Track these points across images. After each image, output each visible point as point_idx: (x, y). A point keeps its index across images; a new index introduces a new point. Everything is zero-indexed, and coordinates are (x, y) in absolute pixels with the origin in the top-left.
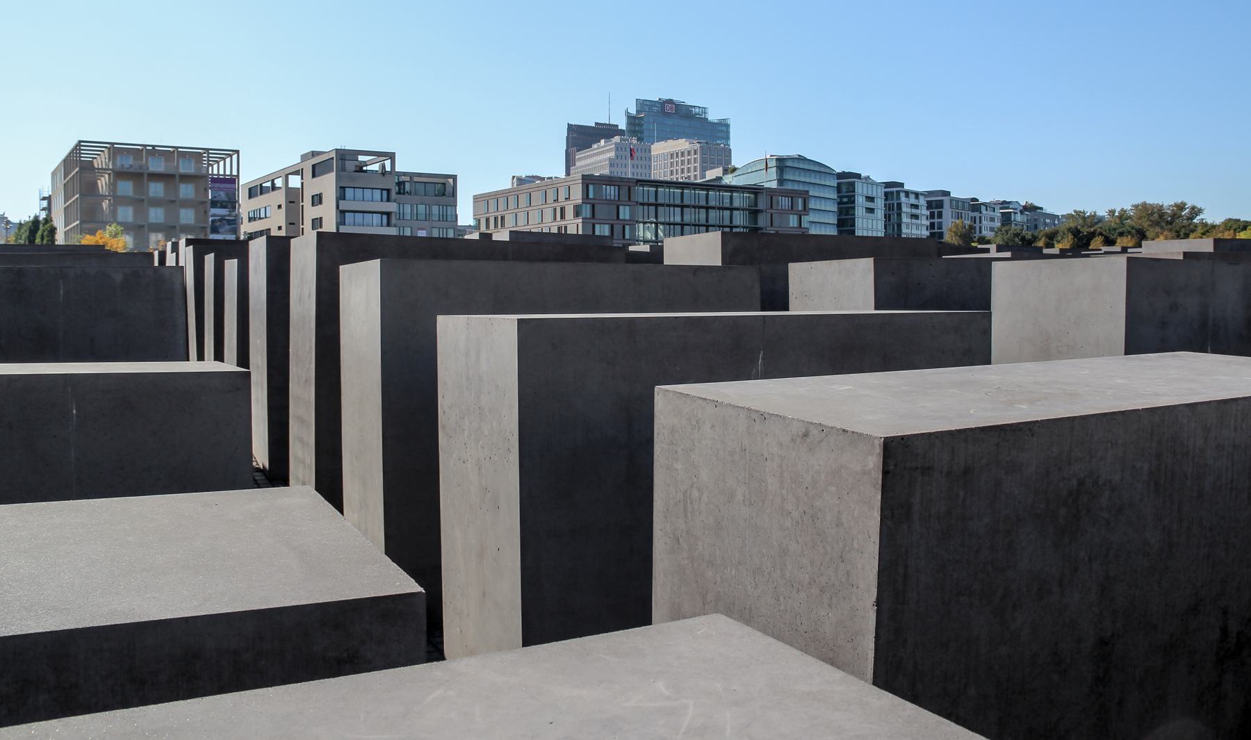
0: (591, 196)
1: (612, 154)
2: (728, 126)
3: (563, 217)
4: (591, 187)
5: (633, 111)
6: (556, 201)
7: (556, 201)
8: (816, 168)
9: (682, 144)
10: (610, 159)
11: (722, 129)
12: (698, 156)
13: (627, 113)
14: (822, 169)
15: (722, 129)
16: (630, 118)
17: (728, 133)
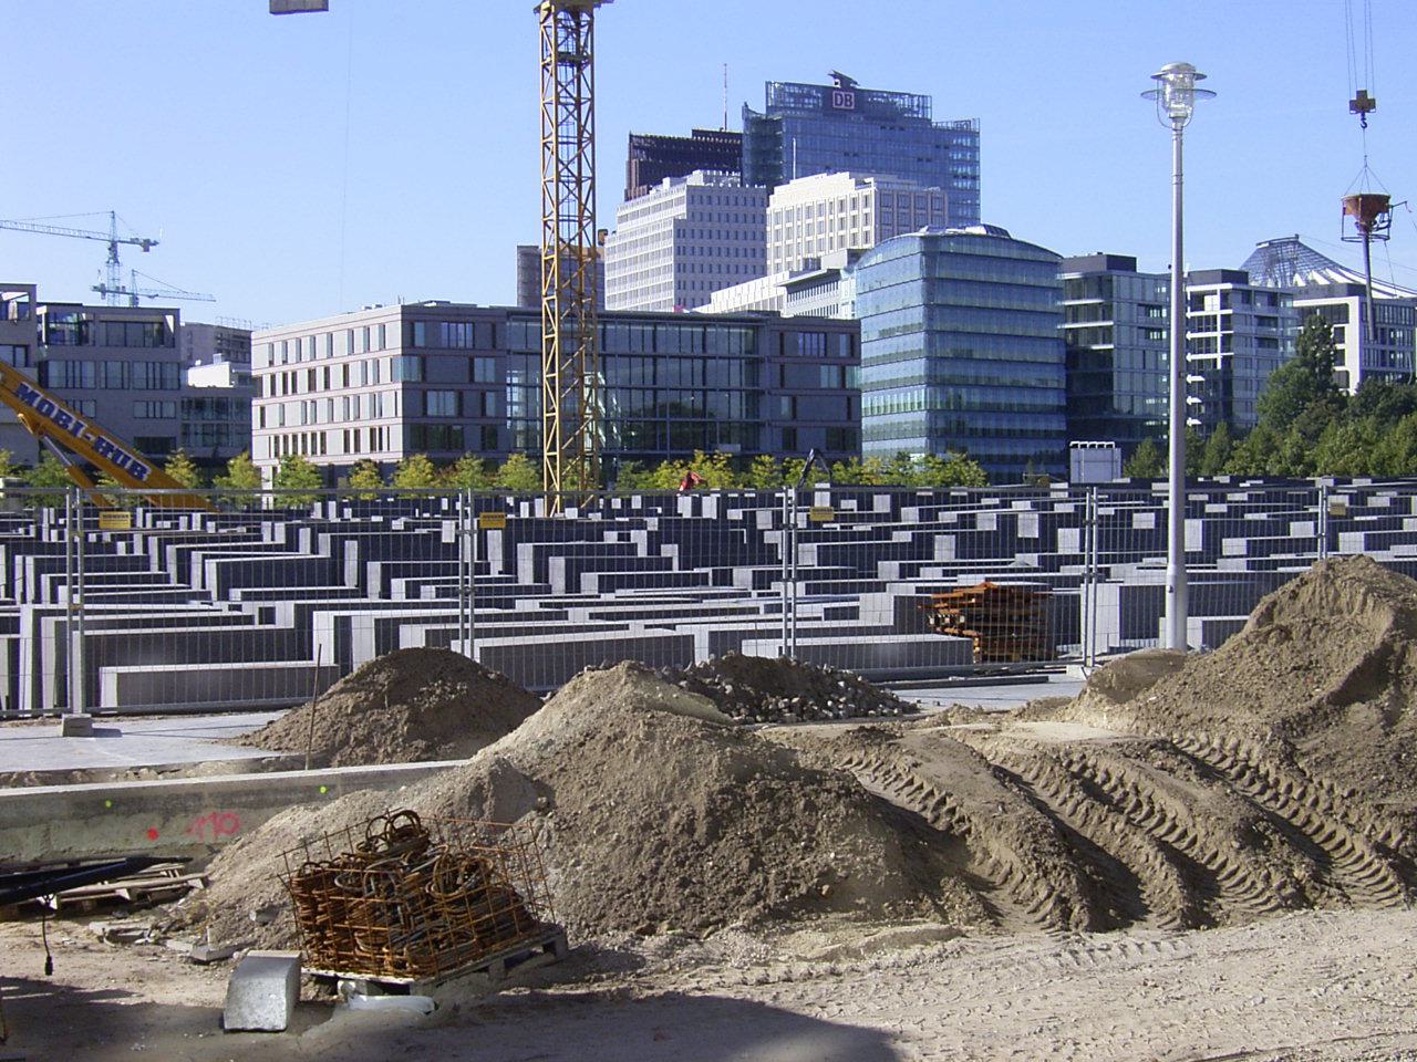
0: (419, 342)
1: (681, 211)
2: (974, 135)
3: (377, 381)
4: (419, 327)
5: (760, 108)
6: (368, 349)
7: (368, 349)
8: (1015, 254)
9: (837, 186)
10: (677, 222)
11: (965, 135)
12: (871, 210)
13: (746, 109)
14: (1029, 255)
15: (965, 135)
16: (752, 120)
17: (975, 149)
